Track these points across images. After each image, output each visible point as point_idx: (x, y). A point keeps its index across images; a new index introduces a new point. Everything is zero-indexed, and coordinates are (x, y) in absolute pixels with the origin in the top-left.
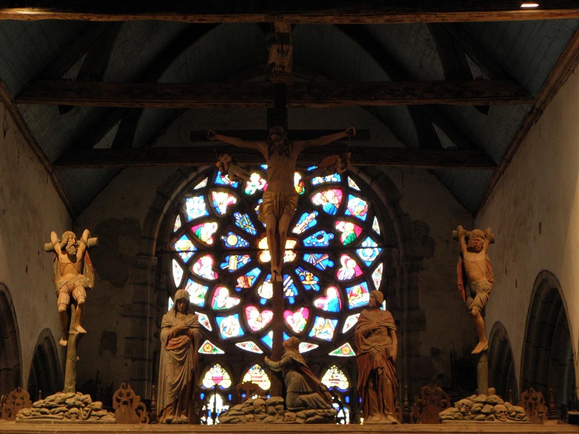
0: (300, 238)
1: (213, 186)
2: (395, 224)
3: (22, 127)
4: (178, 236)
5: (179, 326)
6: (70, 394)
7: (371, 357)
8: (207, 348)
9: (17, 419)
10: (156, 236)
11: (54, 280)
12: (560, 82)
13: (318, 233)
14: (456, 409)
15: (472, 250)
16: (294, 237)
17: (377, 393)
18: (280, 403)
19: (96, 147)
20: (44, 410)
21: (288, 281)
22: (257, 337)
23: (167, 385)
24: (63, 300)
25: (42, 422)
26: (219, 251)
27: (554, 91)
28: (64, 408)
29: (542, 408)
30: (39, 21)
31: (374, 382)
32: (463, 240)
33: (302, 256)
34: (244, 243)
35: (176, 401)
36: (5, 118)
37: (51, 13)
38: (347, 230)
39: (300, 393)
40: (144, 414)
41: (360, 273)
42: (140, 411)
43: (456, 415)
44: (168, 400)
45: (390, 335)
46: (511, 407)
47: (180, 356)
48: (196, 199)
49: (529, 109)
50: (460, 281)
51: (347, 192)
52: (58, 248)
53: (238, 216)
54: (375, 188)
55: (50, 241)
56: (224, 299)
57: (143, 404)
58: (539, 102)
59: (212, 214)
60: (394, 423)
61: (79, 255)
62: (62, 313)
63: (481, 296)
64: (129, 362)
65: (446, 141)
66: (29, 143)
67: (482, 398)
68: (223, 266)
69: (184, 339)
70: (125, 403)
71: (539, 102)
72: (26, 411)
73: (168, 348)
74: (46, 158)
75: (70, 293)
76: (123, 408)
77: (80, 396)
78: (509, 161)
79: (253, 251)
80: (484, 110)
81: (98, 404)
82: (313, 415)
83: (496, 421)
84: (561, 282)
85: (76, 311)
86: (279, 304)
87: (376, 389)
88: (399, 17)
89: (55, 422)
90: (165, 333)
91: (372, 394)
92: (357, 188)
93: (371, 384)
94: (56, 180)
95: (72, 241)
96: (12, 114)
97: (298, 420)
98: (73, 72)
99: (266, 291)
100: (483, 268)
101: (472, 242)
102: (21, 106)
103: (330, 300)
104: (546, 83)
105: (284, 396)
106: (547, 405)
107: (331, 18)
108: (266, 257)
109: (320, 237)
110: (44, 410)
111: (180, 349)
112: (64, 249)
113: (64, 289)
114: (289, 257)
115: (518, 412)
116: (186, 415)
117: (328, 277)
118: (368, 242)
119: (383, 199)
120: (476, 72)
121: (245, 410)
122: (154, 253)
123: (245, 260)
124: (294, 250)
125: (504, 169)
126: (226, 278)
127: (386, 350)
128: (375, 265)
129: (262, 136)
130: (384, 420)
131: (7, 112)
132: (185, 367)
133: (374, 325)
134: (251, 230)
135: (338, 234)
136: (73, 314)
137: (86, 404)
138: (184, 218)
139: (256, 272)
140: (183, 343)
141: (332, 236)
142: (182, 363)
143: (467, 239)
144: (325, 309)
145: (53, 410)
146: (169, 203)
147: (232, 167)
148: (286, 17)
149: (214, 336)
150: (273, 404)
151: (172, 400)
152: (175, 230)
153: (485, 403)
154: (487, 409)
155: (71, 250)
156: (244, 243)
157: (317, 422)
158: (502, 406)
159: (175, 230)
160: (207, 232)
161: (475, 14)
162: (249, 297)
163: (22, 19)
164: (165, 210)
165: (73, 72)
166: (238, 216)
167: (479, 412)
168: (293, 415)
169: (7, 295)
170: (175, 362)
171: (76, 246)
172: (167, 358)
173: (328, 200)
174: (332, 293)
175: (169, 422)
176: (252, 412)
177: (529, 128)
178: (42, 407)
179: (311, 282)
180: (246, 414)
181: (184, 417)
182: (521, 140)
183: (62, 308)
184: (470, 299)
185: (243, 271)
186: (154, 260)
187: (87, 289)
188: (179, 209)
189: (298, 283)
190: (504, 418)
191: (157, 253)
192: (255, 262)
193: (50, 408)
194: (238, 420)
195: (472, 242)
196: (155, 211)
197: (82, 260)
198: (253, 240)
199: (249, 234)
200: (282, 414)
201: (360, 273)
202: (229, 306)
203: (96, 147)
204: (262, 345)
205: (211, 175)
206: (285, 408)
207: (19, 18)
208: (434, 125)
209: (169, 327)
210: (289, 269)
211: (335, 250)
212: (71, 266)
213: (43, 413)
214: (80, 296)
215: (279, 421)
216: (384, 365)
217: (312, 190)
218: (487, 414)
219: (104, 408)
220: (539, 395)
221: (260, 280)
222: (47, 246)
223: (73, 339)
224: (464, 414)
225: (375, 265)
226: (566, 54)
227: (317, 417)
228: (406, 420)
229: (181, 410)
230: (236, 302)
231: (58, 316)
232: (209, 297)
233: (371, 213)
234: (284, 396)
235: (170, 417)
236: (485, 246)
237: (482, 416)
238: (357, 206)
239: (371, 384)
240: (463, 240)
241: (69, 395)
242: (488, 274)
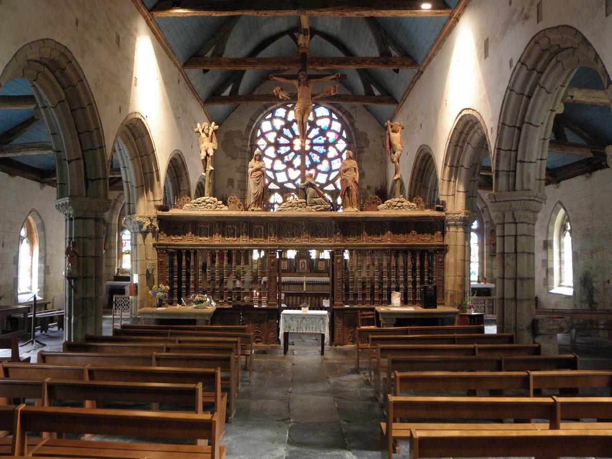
0: (312, 140)
1: (274, 117)
2: (353, 133)
3: (188, 82)
4: (259, 138)
5: (256, 167)
6: (207, 197)
7: (347, 181)
8: (272, 186)
9: (184, 208)
10: (250, 138)
11: (199, 145)
12: (434, 55)
13: (319, 137)
14: (385, 205)
15: (394, 131)
16: (309, 139)
17: (349, 197)
18: (304, 202)
19: (222, 95)
20: (195, 204)
21: (307, 158)
22: (293, 182)
23: (252, 194)
24: (203, 154)
25: (195, 210)
26: (277, 145)
27: (430, 60)
28: (205, 204)
29: (422, 205)
30: (188, 17)
31: (348, 193)
32: (390, 127)
33: (312, 147)
34: (287, 142)
35: (256, 201)
36: (179, 75)
37: (193, 12)
38: (332, 136)
39: (314, 198)
40: (242, 207)
41: (337, 154)
42: (240, 206)
43: (385, 207)
44: (252, 201)
45: (355, 171)
46: (410, 204)
47: (258, 180)
48: (266, 122)
49: (417, 72)
50: (388, 146)
51: (332, 119)
52: (200, 131)
53: (284, 130)
54: (344, 118)
55: (197, 127)
56: (279, 165)
57: (241, 203)
58: (422, 67)
59: (274, 129)
60: (357, 211)
61: (210, 134)
62: (203, 160)
63: (398, 153)
64: (239, 191)
65: (377, 93)
66: (192, 90)
67: (397, 199)
68: (279, 151)
69: (259, 173)
70: (233, 202)
71: (422, 67)
72: (188, 205)
73: (252, 177)
74: (200, 99)
75: (206, 151)
76: (232, 205)
77: (212, 198)
78: (405, 100)
79: (291, 145)
80: (397, 71)
81: (220, 202)
82: (319, 208)
83: (403, 210)
84: (432, 149)
85: (209, 159)
86: (302, 168)
87: (348, 196)
88: (363, 12)
90: (250, 170)
91: (347, 198)
92: (336, 118)
93: (346, 194)
94: (205, 110)
95: (207, 127)
96: (182, 74)
97: (312, 210)
98: (209, 54)
99: (297, 162)
100: (399, 140)
101: (394, 128)
102: (187, 70)
103: (324, 166)
104: (427, 56)
105: (306, 199)
106: (425, 203)
107: (329, 12)
108: (297, 147)
109: (320, 139)
110: (195, 204)
111: (257, 177)
112: (203, 131)
113: (204, 149)
114: (307, 148)
115: (413, 206)
116: (261, 207)
117: (323, 156)
118: (341, 141)
119: (348, 123)
120: (394, 53)
121: (288, 205)
122: (249, 145)
123: (288, 148)
124: (309, 145)
125: (402, 105)
126: (280, 157)
127: (354, 178)
128: (343, 151)
129: (295, 77)
130: (352, 210)
131: (180, 72)
132: (259, 186)
133: (348, 167)
134: (291, 136)
135: (328, 138)
136: (208, 161)
137: (215, 202)
138: (261, 131)
139: (293, 154)
140: (259, 174)
141: (325, 139)
142: (258, 184)
143: (391, 127)
144: (322, 170)
146: (255, 124)
147: (281, 92)
148: (307, 12)
149: (275, 181)
150: (301, 203)
151: (254, 201)
152: (258, 136)
153: (398, 202)
154: (399, 204)
155: (206, 131)
156: (287, 142)
157: (321, 210)
158: (406, 203)
159: (258, 136)
160: (272, 137)
161: (399, 12)
162: (290, 164)
163: (180, 16)
164: (253, 127)
165: (209, 54)
166: (284, 130)
167: (396, 206)
168: (311, 207)
169: (182, 156)
170: (255, 183)
171: (209, 129)
172: (251, 181)
173: (323, 123)
174: (325, 162)
175: (253, 210)
176: (291, 206)
177: (415, 82)
178: (195, 203)
179: (316, 158)
180: (288, 207)
181: (259, 208)
182: (411, 89)
183: (203, 158)
184: (393, 154)
185: (287, 153)
186: (249, 148)
187: (214, 149)
188: (259, 127)
189: (311, 159)
190: (407, 208)
191: (250, 145)
192: (292, 150)
193: (198, 203)
195: (394, 128)
196: (249, 127)
197: (212, 136)
198: (291, 140)
199: (289, 138)
200: (304, 207)
201: (337, 154)
202: (281, 169)
203: (222, 95)
204: (295, 185)
205: (273, 111)
206: (307, 205)
207: (178, 15)
208: (372, 86)
209: (252, 167)
210: (307, 153)
211: (326, 145)
212: (206, 138)
213: (196, 206)
214: (211, 152)
215: (304, 210)
216: (353, 185)
217: (316, 118)
218: (399, 207)
219: (223, 203)
220: (421, 199)
221: (294, 157)
222: (196, 130)
223: (208, 172)
224: (389, 207)
225: (343, 151)
226: (439, 38)
227: (321, 208)
228: (361, 210)
229: (258, 205)
230: (284, 166)
231: (201, 162)
232: (273, 164)
233: (342, 129)
234: (306, 199)
235: (253, 208)
236: (400, 130)
237: (397, 208)
238: (337, 126)
239: (346, 194)
240: (390, 127)
241: (207, 198)
242: (401, 143)
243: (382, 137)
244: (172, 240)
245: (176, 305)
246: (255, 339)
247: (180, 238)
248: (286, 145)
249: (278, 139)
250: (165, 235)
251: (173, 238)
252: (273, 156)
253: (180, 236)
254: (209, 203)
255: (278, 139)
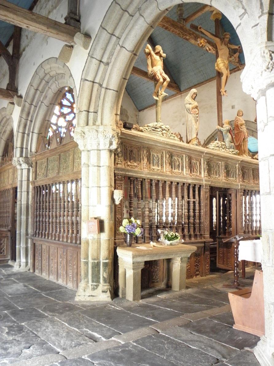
34: (69, 105)
89: (159, 136)
123: (69, 110)
145: (157, 130)
157: (234, 154)
166: (67, 94)
185: (69, 114)
192: (72, 112)
194: (215, 149)
243: (137, 115)
244: (128, 165)
245: (149, 243)
246: (196, 272)
247: (135, 164)
248: (68, 107)
249: (62, 101)
250: (122, 159)
251: (129, 163)
252: (58, 114)
253: (135, 162)
254: (165, 130)
255: (62, 101)
